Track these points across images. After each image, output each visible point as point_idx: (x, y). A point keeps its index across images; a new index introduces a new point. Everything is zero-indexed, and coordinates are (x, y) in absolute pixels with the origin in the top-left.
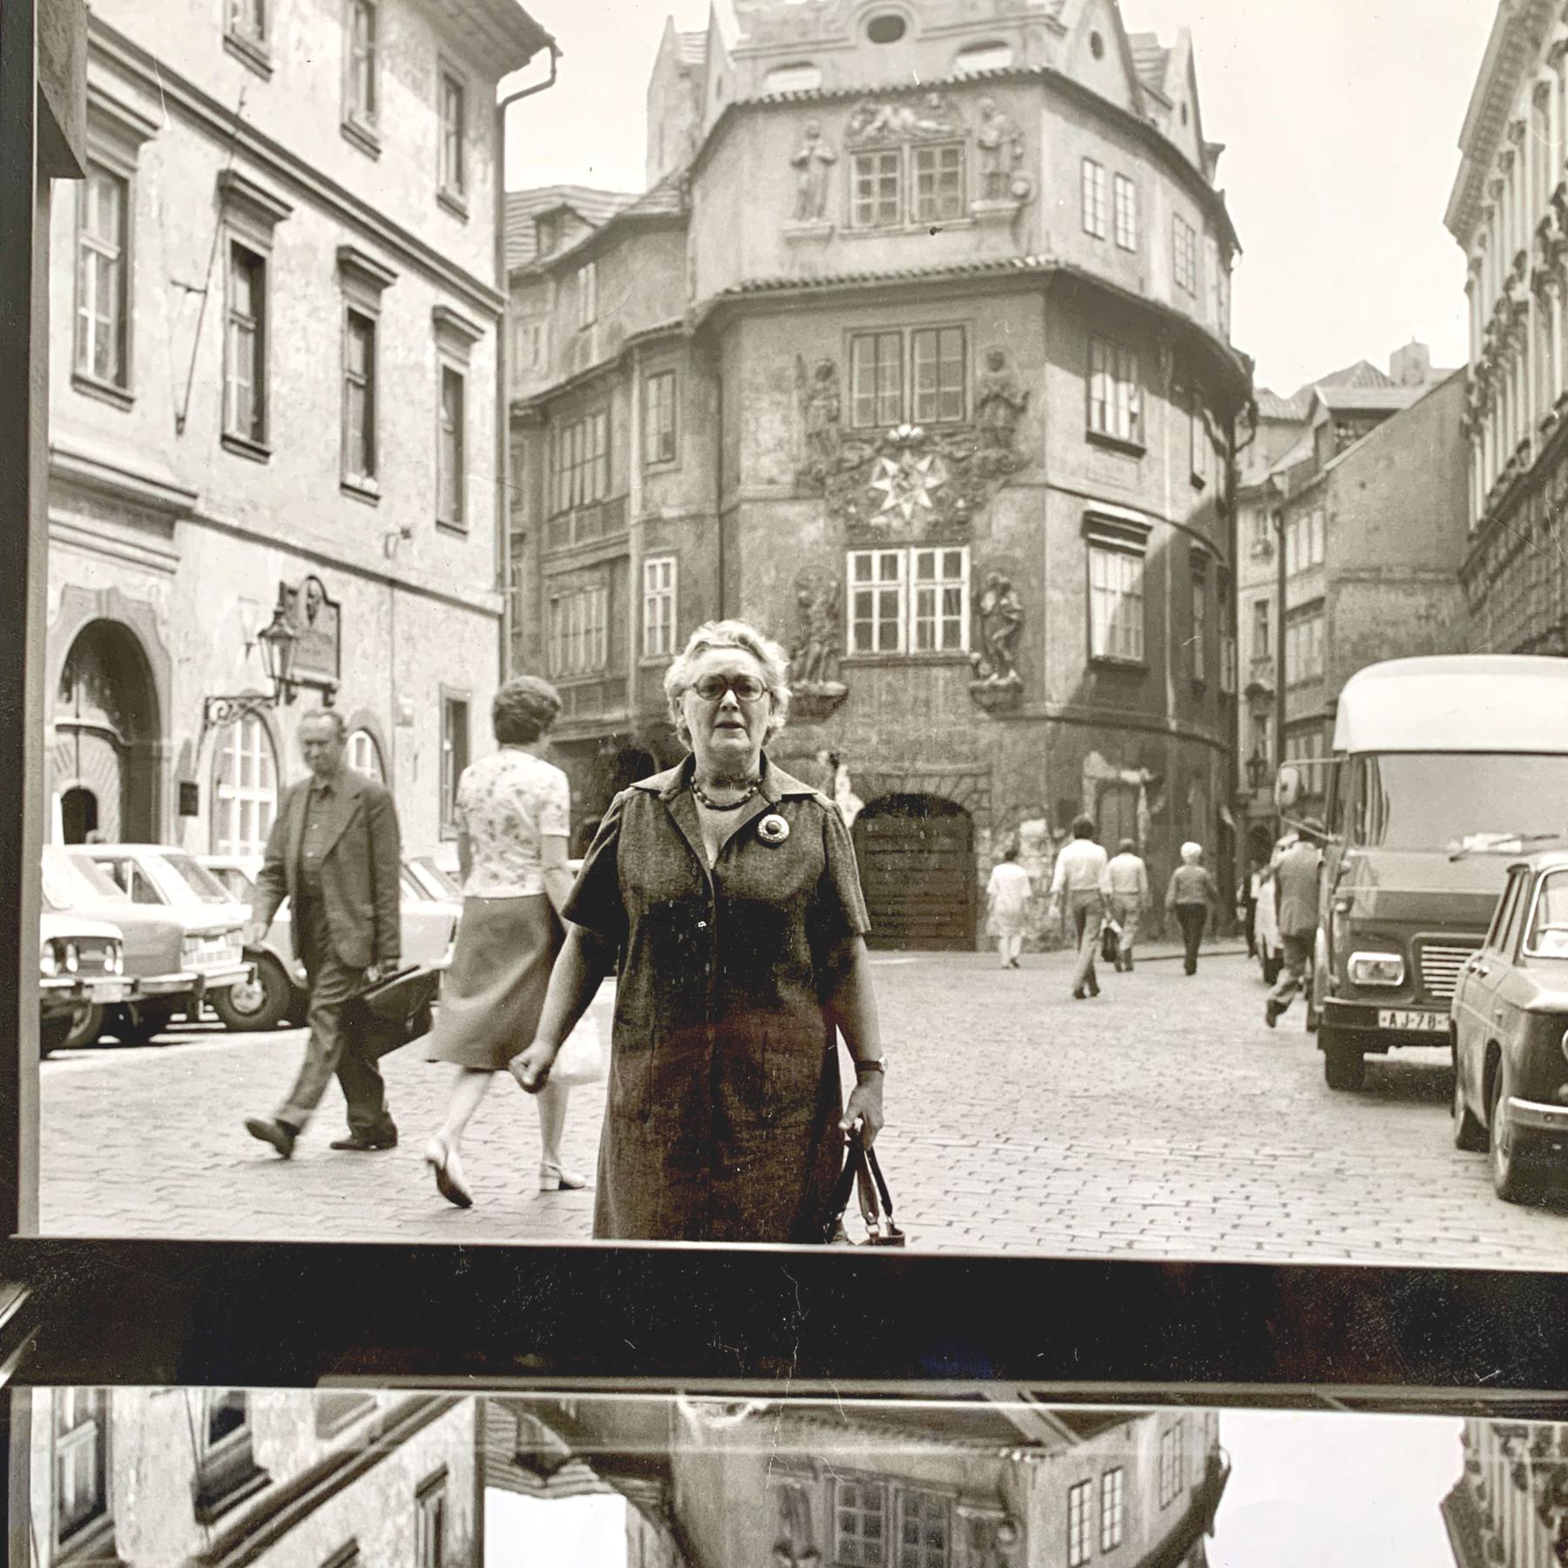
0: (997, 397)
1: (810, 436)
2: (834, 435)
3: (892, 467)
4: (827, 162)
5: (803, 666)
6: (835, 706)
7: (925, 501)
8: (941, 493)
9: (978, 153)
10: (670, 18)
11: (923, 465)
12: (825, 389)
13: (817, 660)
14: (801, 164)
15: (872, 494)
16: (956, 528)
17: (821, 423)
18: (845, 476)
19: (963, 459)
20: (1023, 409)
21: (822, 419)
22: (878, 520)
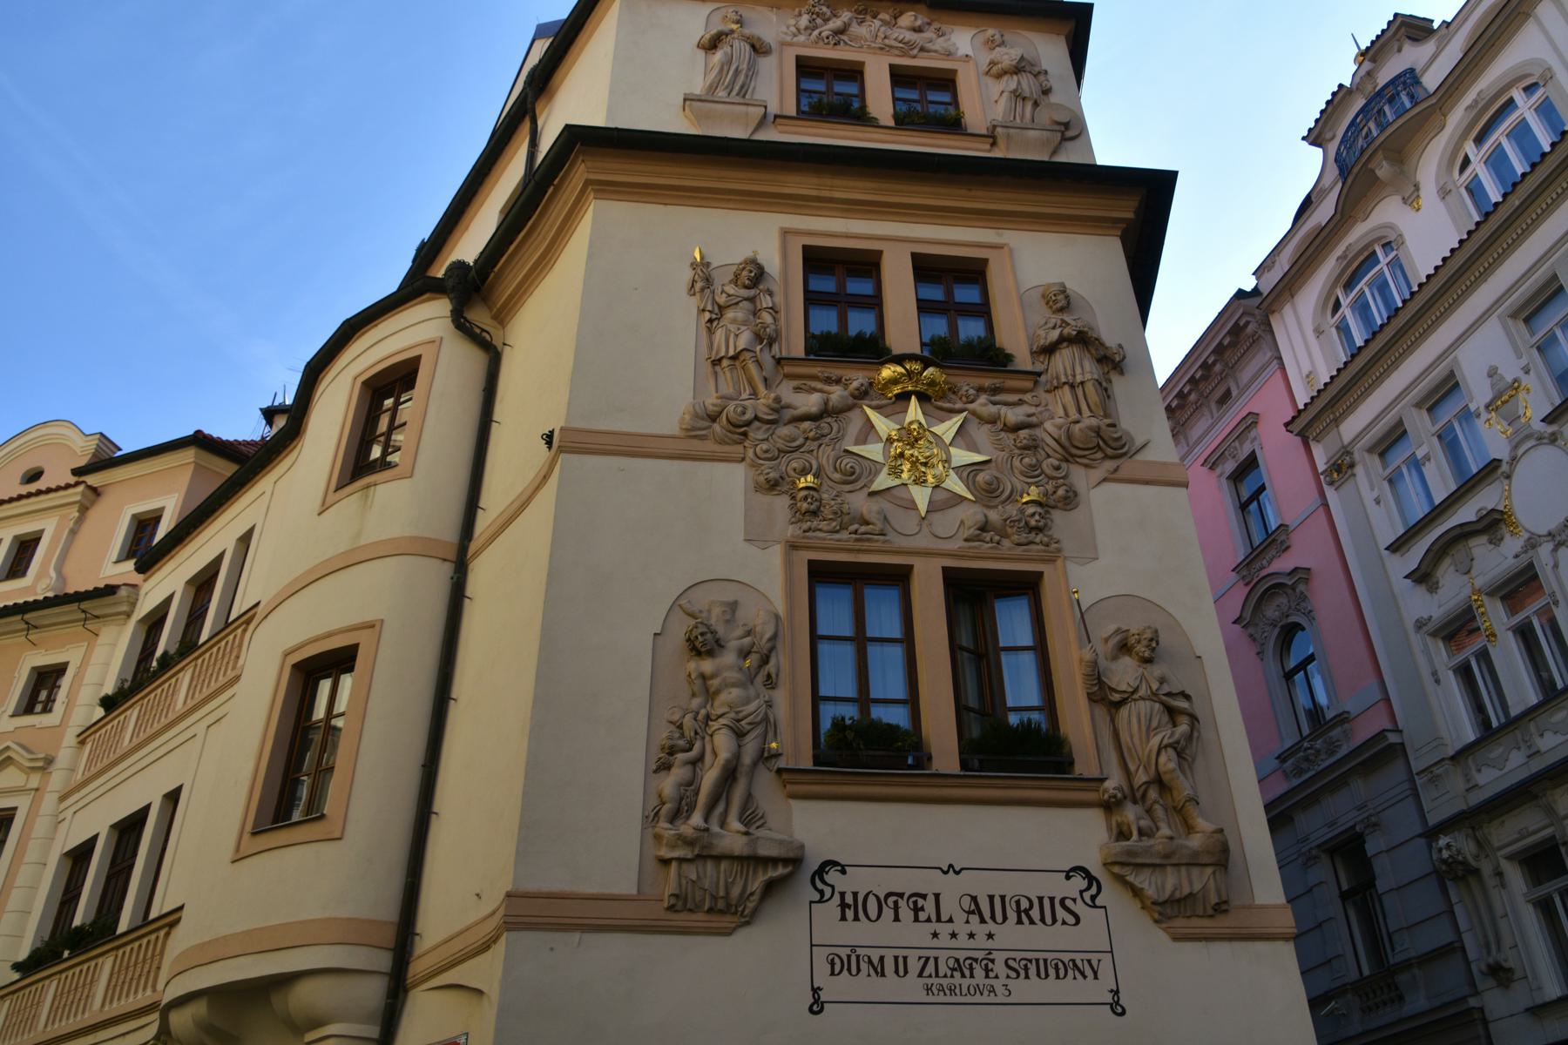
1: (716, 362)
2: (767, 359)
3: (883, 425)
4: (758, 48)
5: (691, 784)
6: (771, 887)
7: (955, 485)
9: (989, 81)
10: (319, 514)
11: (947, 429)
12: (752, 300)
13: (730, 775)
14: (712, 44)
15: (847, 462)
16: (1023, 537)
22: (858, 502)
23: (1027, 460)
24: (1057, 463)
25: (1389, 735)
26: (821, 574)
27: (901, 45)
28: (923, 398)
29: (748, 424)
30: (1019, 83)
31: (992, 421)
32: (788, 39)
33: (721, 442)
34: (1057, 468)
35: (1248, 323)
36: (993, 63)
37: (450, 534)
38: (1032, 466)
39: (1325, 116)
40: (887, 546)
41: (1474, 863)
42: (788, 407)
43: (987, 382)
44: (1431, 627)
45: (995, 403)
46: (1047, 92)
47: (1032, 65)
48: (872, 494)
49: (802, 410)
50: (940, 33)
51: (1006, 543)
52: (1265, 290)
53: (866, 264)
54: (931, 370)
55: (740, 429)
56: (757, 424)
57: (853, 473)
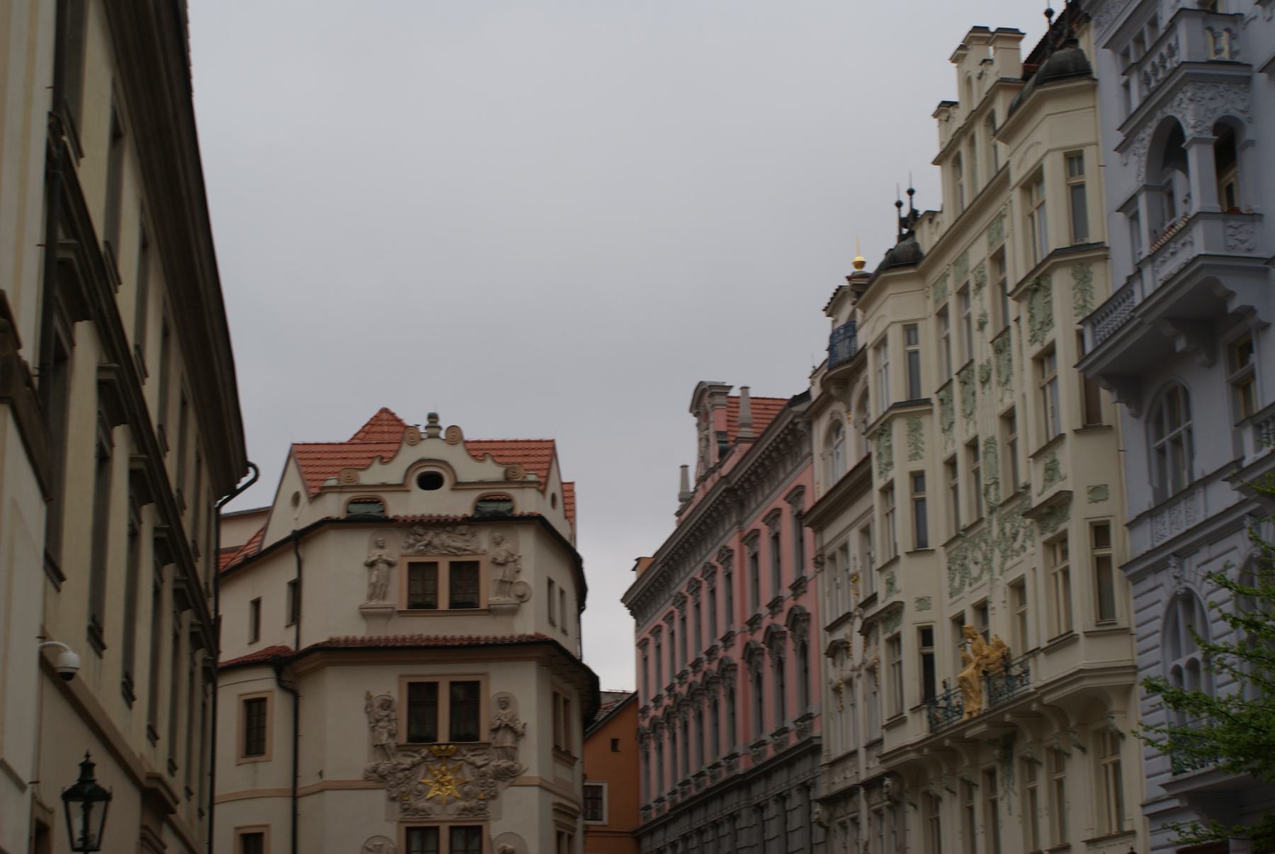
0: (507, 725)
1: (376, 746)
2: (392, 743)
4: (390, 564)
8: (466, 788)
12: (387, 716)
14: (371, 565)
15: (420, 787)
16: (478, 812)
17: (384, 739)
18: (400, 775)
19: (482, 766)
20: (523, 735)
21: (385, 736)
23: (483, 781)
24: (491, 780)
25: (814, 740)
26: (409, 830)
27: (454, 551)
28: (448, 757)
29: (386, 775)
30: (505, 572)
31: (472, 764)
32: (404, 552)
33: (376, 781)
34: (492, 783)
35: (798, 423)
36: (495, 559)
37: (289, 785)
38: (483, 784)
39: (833, 302)
40: (431, 820)
41: (827, 824)
42: (399, 764)
43: (472, 747)
44: (833, 685)
45: (473, 756)
46: (518, 572)
47: (513, 555)
48: (428, 800)
49: (405, 766)
50: (474, 535)
51: (471, 815)
52: (815, 393)
53: (432, 687)
54: (451, 746)
55: (383, 777)
56: (389, 774)
57: (420, 792)
